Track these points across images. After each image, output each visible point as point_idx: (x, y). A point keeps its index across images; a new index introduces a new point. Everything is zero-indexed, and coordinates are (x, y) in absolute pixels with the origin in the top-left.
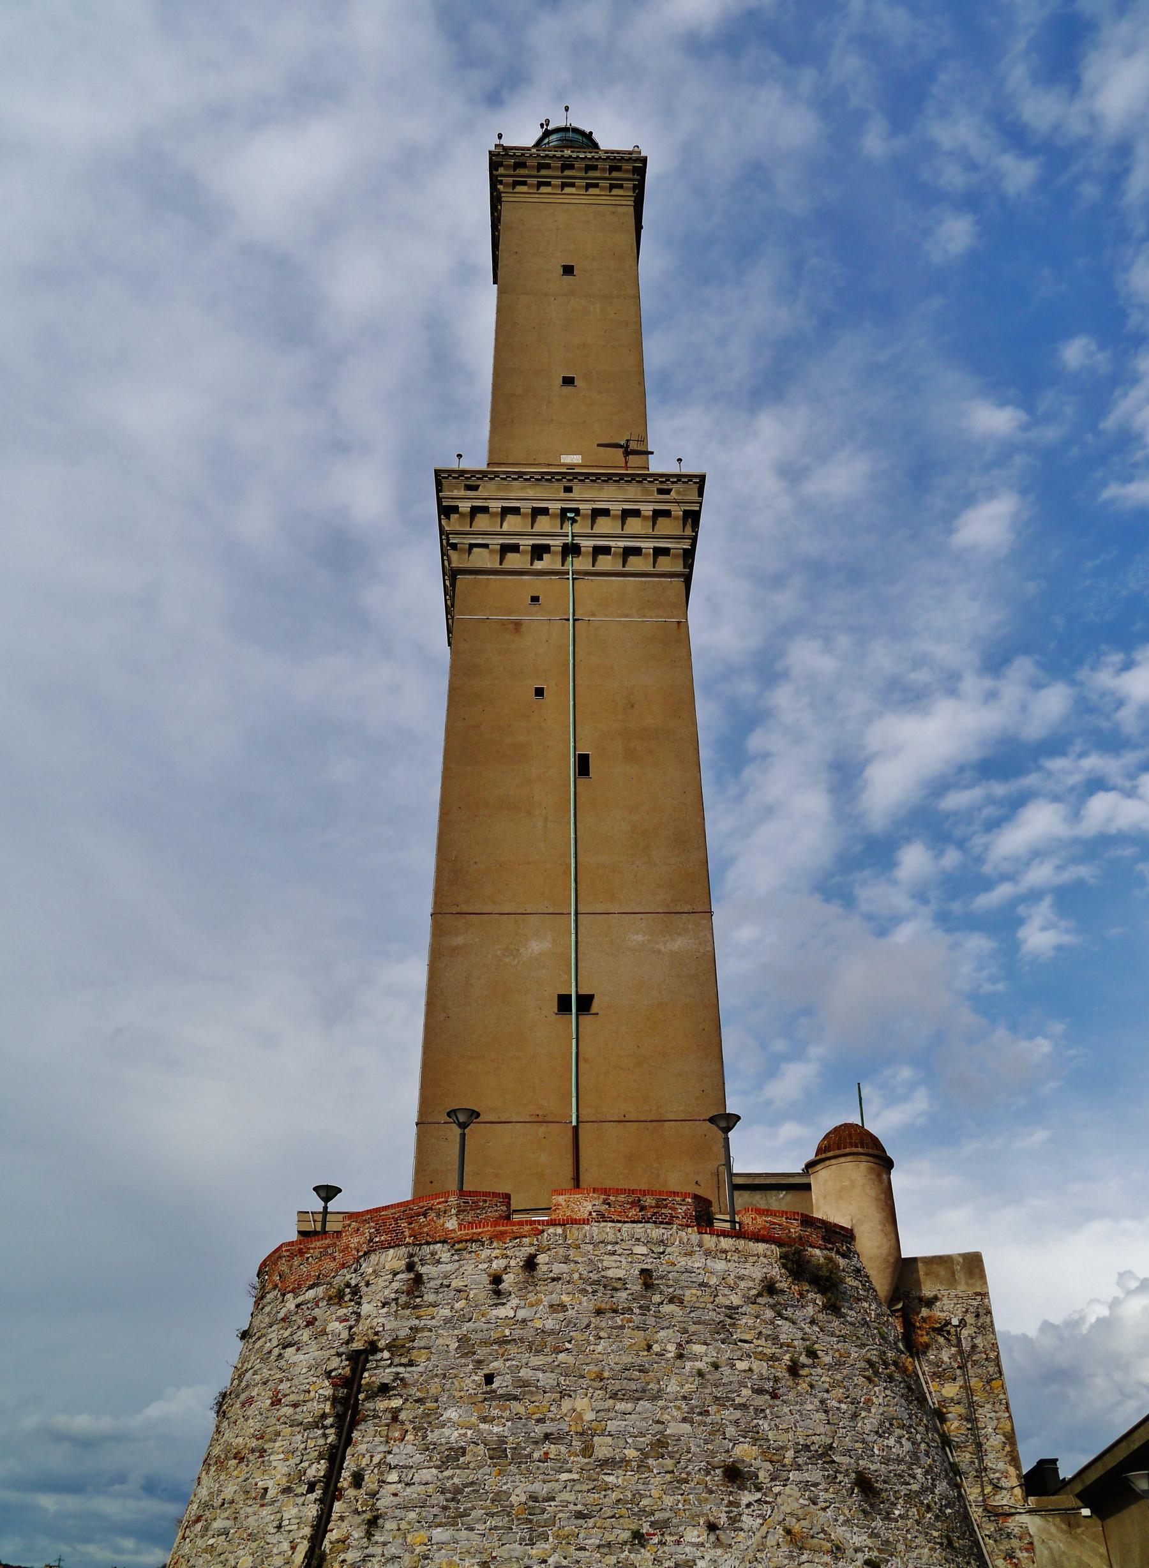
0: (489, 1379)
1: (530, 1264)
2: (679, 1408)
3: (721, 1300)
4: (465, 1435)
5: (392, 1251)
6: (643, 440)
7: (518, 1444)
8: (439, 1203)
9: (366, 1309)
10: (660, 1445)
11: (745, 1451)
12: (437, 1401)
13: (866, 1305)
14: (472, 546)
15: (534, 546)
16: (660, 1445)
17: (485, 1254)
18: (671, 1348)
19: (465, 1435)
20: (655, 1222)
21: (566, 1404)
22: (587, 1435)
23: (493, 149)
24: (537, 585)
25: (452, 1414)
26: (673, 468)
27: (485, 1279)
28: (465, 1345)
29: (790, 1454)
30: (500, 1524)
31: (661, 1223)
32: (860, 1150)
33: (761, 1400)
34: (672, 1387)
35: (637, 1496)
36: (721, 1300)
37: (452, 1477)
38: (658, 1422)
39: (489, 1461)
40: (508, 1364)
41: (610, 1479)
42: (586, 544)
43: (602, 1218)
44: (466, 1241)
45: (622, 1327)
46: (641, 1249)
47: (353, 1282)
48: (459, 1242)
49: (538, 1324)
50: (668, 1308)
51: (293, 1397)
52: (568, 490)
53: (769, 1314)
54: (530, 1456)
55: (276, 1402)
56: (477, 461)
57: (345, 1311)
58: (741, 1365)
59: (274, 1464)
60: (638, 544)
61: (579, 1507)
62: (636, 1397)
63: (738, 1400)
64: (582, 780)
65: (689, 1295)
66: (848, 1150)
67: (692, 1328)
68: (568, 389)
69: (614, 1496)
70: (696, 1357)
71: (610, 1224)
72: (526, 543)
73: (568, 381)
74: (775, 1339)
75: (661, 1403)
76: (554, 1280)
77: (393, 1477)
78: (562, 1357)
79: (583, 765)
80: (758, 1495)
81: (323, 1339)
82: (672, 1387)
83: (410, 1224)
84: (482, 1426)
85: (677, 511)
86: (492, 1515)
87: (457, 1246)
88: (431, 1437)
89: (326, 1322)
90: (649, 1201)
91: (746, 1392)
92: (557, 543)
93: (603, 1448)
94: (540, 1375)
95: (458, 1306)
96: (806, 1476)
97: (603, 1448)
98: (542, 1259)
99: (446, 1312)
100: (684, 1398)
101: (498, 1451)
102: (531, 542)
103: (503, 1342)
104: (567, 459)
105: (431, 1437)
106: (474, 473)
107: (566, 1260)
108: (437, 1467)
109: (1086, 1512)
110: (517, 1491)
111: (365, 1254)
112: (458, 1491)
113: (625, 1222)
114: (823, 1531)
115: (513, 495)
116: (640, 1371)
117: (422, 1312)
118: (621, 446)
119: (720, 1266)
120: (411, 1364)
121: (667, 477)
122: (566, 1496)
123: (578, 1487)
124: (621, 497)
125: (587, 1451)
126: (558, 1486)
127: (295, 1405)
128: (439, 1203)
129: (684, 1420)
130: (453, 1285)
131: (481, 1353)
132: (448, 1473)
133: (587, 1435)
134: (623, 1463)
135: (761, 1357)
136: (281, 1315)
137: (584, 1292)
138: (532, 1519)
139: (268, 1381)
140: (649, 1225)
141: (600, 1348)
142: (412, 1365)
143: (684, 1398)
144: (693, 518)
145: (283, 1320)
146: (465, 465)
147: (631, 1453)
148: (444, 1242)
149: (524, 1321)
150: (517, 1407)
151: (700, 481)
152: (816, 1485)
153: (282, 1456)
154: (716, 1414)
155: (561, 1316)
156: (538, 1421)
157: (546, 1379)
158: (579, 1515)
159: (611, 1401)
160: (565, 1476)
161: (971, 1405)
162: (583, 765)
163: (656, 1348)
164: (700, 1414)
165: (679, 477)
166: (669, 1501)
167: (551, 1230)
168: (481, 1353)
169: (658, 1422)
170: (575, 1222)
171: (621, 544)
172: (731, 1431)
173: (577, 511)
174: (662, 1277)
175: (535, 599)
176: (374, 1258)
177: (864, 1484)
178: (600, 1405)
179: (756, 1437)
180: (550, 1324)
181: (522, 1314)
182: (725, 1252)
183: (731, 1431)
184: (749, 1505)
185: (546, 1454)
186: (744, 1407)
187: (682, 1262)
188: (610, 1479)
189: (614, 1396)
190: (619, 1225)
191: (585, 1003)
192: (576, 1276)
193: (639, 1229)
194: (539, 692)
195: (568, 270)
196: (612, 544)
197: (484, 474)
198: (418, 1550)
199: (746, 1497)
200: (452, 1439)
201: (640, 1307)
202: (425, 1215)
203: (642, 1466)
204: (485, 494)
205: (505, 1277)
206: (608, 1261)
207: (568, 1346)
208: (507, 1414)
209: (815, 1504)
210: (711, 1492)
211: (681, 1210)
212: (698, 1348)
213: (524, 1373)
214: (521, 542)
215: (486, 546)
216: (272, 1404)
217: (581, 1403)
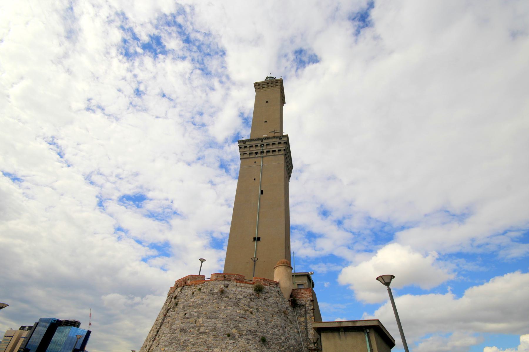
0: (186, 314)
1: (200, 289)
11: (234, 331)
16: (214, 329)
18: (223, 307)
24: (255, 160)
27: (191, 293)
28: (184, 307)
29: (245, 332)
35: (206, 340)
41: (201, 336)
42: (265, 151)
53: (249, 300)
58: (238, 311)
62: (211, 318)
64: (262, 195)
65: (230, 296)
67: (229, 303)
70: (228, 309)
72: (254, 152)
74: (249, 306)
79: (262, 192)
82: (221, 316)
85: (282, 142)
88: (172, 327)
91: (238, 317)
96: (248, 337)
97: (202, 330)
98: (202, 288)
99: (183, 300)
107: (207, 289)
119: (240, 289)
122: (191, 340)
125: (199, 330)
126: (190, 338)
133: (199, 327)
137: (208, 295)
147: (207, 331)
154: (230, 322)
157: (195, 314)
158: (193, 345)
161: (306, 323)
162: (262, 192)
166: (213, 342)
168: (186, 308)
172: (232, 326)
177: (264, 340)
178: (204, 320)
179: (237, 327)
183: (232, 326)
186: (236, 321)
188: (201, 336)
191: (259, 239)
194: (255, 179)
195: (267, 102)
199: (232, 341)
211: (233, 278)
213: (192, 313)
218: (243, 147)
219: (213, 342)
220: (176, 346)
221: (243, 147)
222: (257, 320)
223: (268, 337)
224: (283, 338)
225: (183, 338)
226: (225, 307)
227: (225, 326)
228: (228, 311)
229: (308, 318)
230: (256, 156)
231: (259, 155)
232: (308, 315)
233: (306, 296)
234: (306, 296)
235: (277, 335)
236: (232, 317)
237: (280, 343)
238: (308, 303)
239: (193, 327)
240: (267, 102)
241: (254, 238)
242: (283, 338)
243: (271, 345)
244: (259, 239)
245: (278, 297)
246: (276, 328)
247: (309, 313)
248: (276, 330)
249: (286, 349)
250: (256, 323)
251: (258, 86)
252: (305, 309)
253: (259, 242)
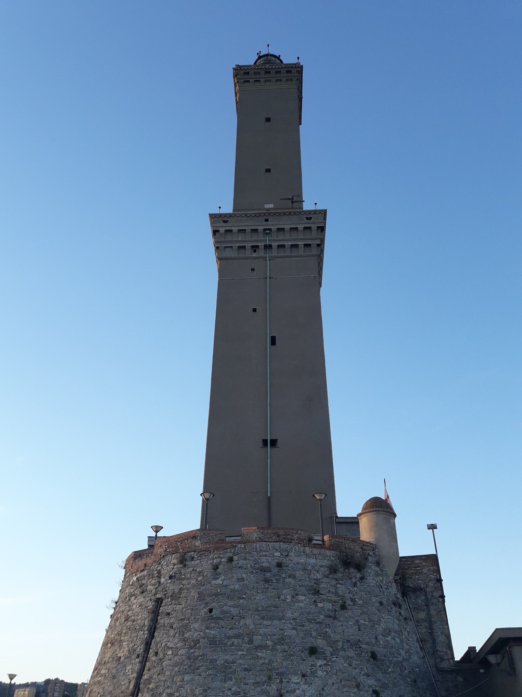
0: (211, 611)
1: (231, 560)
2: (291, 624)
3: (312, 576)
4: (200, 634)
5: (174, 555)
6: (300, 195)
7: (222, 638)
9: (162, 580)
10: (282, 640)
11: (320, 643)
12: (189, 620)
13: (381, 578)
15: (252, 247)
16: (282, 640)
19: (200, 634)
20: (284, 542)
21: (242, 622)
22: (251, 635)
23: (235, 67)
25: (196, 625)
26: (312, 208)
28: (201, 596)
31: (287, 542)
32: (380, 509)
33: (328, 621)
34: (289, 615)
35: (271, 662)
36: (312, 576)
38: (282, 629)
40: (219, 604)
41: (260, 654)
42: (275, 244)
43: (261, 540)
44: (204, 551)
45: (268, 588)
46: (278, 554)
47: (158, 569)
48: (201, 551)
49: (232, 587)
50: (288, 580)
51: (133, 618)
52: (267, 220)
53: (334, 582)
54: (226, 644)
55: (127, 620)
56: (228, 208)
57: (154, 581)
58: (320, 605)
60: (297, 243)
61: (246, 666)
62: (271, 619)
63: (318, 620)
64: (273, 347)
65: (299, 574)
66: (374, 509)
68: (268, 174)
69: (261, 661)
70: (299, 601)
71: (265, 543)
72: (248, 245)
73: (268, 171)
74: (336, 594)
75: (283, 621)
76: (239, 567)
77: (170, 652)
78: (241, 601)
80: (325, 662)
81: (145, 594)
82: (289, 615)
83: (181, 543)
84: (207, 631)
85: (314, 227)
86: (209, 669)
87: (200, 553)
88: (186, 635)
89: (147, 586)
90: (281, 532)
91: (322, 617)
92: (262, 244)
93: (257, 640)
94: (232, 609)
95: (199, 579)
97: (257, 640)
98: (235, 558)
99: (193, 582)
100: (294, 619)
101: (213, 642)
102: (251, 245)
103: (217, 595)
104: (267, 206)
105: (186, 635)
106: (226, 215)
107: (245, 559)
109: (482, 671)
110: (220, 659)
111: (163, 556)
112: (196, 658)
113: (271, 542)
114: (354, 678)
115: (243, 224)
116: (275, 607)
117: (184, 582)
118: (290, 199)
119: (313, 561)
120: (179, 604)
121: (310, 212)
122: (241, 661)
123: (246, 657)
124: (289, 223)
125: (251, 642)
127: (134, 621)
129: (293, 629)
130: (198, 570)
131: (208, 599)
133: (251, 635)
134: (266, 647)
135: (330, 601)
136: (131, 583)
137: (252, 573)
138: (226, 671)
139: (124, 611)
140: (281, 543)
141: (258, 598)
142: (180, 605)
143: (294, 619)
144: (322, 229)
145: (132, 585)
146: (223, 211)
147: (269, 643)
148: (195, 551)
149: (226, 586)
150: (222, 623)
151: (324, 213)
152: (351, 658)
154: (309, 626)
155: (242, 583)
156: (231, 629)
157: (235, 611)
158: (246, 670)
159: (262, 620)
160: (240, 653)
161: (431, 623)
163: (282, 597)
164: (300, 626)
165: (315, 212)
166: (285, 664)
167: (239, 546)
169: (282, 629)
170: (249, 542)
171: (290, 243)
172: (314, 634)
173: (270, 229)
174: (286, 566)
176: (167, 558)
179: (325, 636)
180: (237, 587)
181: (225, 583)
182: (315, 555)
183: (314, 634)
184: (321, 666)
185: (233, 643)
186: (320, 623)
187: (296, 559)
189: (263, 618)
190: (269, 543)
191: (274, 443)
192: (249, 566)
193: (277, 545)
194: (255, 310)
195: (268, 120)
196: (285, 243)
197: (230, 215)
199: (320, 662)
200: (194, 636)
201: (276, 580)
203: (274, 649)
204: (231, 225)
205: (219, 566)
206: (263, 559)
207: (244, 596)
208: (217, 626)
209: (350, 666)
210: (304, 660)
211: (296, 537)
212: (302, 598)
214: (246, 245)
216: (125, 621)
217: (249, 621)
218: (222, 230)
219: (285, 664)
220: (210, 672)
221: (222, 230)
222: (357, 621)
223: (379, 651)
224: (403, 653)
225: (221, 658)
226: (293, 597)
227: (301, 634)
228: (301, 604)
229: (433, 612)
230: (254, 255)
231: (261, 253)
232: (432, 607)
233: (425, 571)
234: (425, 571)
235: (392, 647)
236: (310, 617)
237: (401, 662)
238: (431, 584)
239: (238, 636)
240: (268, 120)
241: (265, 442)
242: (403, 653)
243: (389, 667)
244: (274, 443)
245: (380, 575)
246: (390, 635)
247: (432, 604)
248: (389, 638)
249: (410, 672)
250: (356, 627)
251: (242, 74)
252: (426, 595)
253: (275, 449)
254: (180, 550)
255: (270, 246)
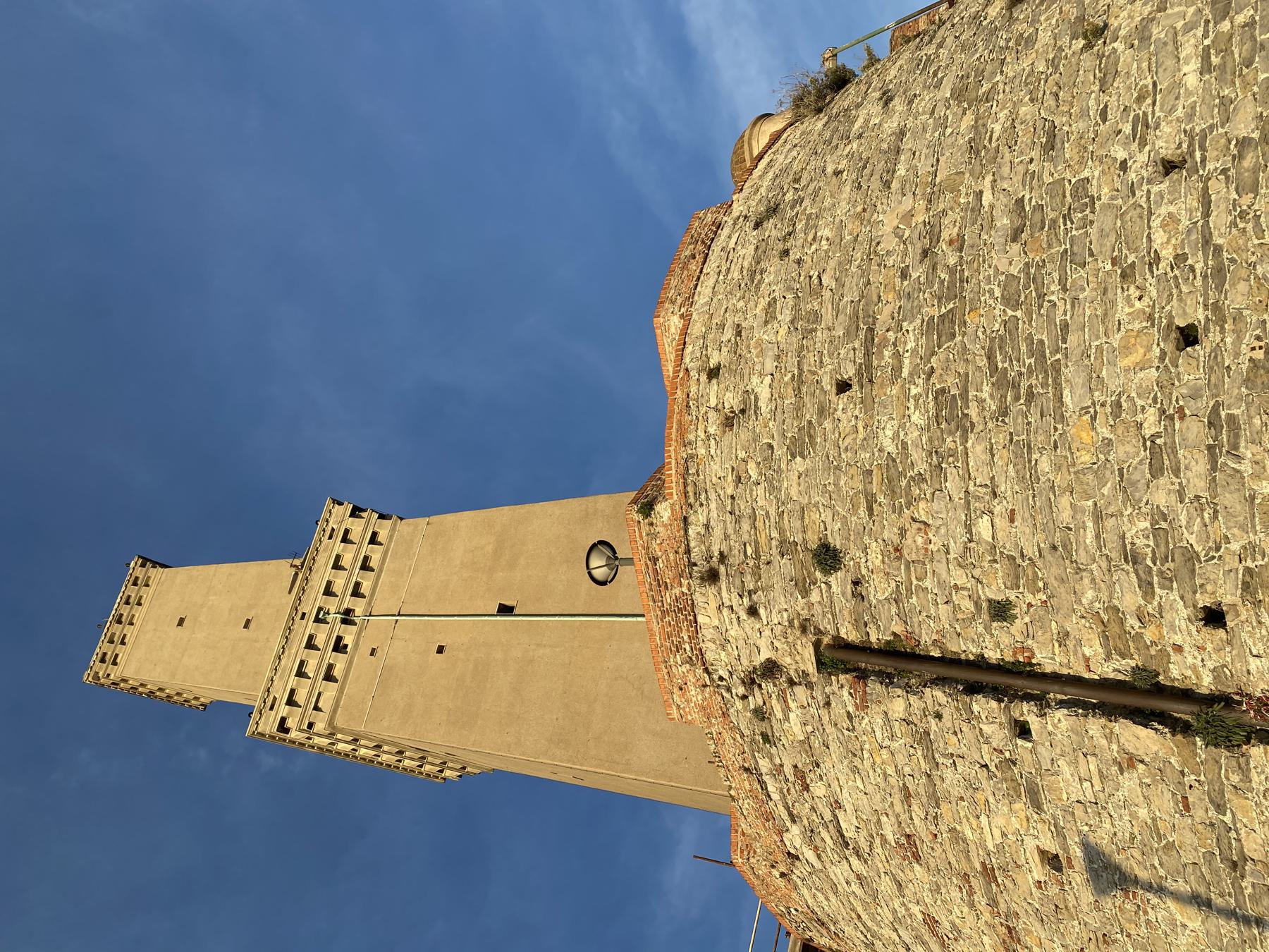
0: (843, 387)
4: (917, 398)
5: (700, 619)
8: (641, 537)
14: (316, 708)
17: (702, 451)
30: (1056, 275)
31: (715, 233)
37: (981, 401)
39: (958, 338)
43: (690, 300)
44: (685, 485)
48: (686, 493)
54: (951, 271)
59: (997, 833)
64: (516, 611)
68: (252, 625)
101: (942, 329)
105: (922, 467)
108: (965, 440)
128: (641, 537)
130: (730, 491)
131: (810, 414)
132: (973, 412)
153: (983, 818)
160: (987, 198)
167: (687, 360)
173: (320, 609)
175: (373, 652)
195: (181, 622)
198: (1105, 432)
202: (655, 560)
204: (281, 690)
215: (320, 694)
240: (181, 622)
254: (685, 589)
255: (348, 612)
